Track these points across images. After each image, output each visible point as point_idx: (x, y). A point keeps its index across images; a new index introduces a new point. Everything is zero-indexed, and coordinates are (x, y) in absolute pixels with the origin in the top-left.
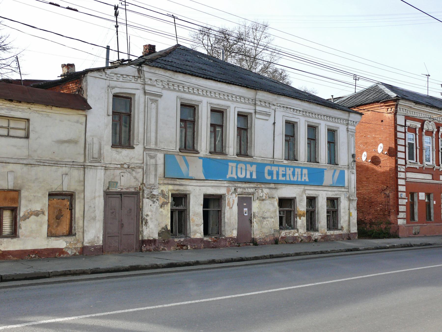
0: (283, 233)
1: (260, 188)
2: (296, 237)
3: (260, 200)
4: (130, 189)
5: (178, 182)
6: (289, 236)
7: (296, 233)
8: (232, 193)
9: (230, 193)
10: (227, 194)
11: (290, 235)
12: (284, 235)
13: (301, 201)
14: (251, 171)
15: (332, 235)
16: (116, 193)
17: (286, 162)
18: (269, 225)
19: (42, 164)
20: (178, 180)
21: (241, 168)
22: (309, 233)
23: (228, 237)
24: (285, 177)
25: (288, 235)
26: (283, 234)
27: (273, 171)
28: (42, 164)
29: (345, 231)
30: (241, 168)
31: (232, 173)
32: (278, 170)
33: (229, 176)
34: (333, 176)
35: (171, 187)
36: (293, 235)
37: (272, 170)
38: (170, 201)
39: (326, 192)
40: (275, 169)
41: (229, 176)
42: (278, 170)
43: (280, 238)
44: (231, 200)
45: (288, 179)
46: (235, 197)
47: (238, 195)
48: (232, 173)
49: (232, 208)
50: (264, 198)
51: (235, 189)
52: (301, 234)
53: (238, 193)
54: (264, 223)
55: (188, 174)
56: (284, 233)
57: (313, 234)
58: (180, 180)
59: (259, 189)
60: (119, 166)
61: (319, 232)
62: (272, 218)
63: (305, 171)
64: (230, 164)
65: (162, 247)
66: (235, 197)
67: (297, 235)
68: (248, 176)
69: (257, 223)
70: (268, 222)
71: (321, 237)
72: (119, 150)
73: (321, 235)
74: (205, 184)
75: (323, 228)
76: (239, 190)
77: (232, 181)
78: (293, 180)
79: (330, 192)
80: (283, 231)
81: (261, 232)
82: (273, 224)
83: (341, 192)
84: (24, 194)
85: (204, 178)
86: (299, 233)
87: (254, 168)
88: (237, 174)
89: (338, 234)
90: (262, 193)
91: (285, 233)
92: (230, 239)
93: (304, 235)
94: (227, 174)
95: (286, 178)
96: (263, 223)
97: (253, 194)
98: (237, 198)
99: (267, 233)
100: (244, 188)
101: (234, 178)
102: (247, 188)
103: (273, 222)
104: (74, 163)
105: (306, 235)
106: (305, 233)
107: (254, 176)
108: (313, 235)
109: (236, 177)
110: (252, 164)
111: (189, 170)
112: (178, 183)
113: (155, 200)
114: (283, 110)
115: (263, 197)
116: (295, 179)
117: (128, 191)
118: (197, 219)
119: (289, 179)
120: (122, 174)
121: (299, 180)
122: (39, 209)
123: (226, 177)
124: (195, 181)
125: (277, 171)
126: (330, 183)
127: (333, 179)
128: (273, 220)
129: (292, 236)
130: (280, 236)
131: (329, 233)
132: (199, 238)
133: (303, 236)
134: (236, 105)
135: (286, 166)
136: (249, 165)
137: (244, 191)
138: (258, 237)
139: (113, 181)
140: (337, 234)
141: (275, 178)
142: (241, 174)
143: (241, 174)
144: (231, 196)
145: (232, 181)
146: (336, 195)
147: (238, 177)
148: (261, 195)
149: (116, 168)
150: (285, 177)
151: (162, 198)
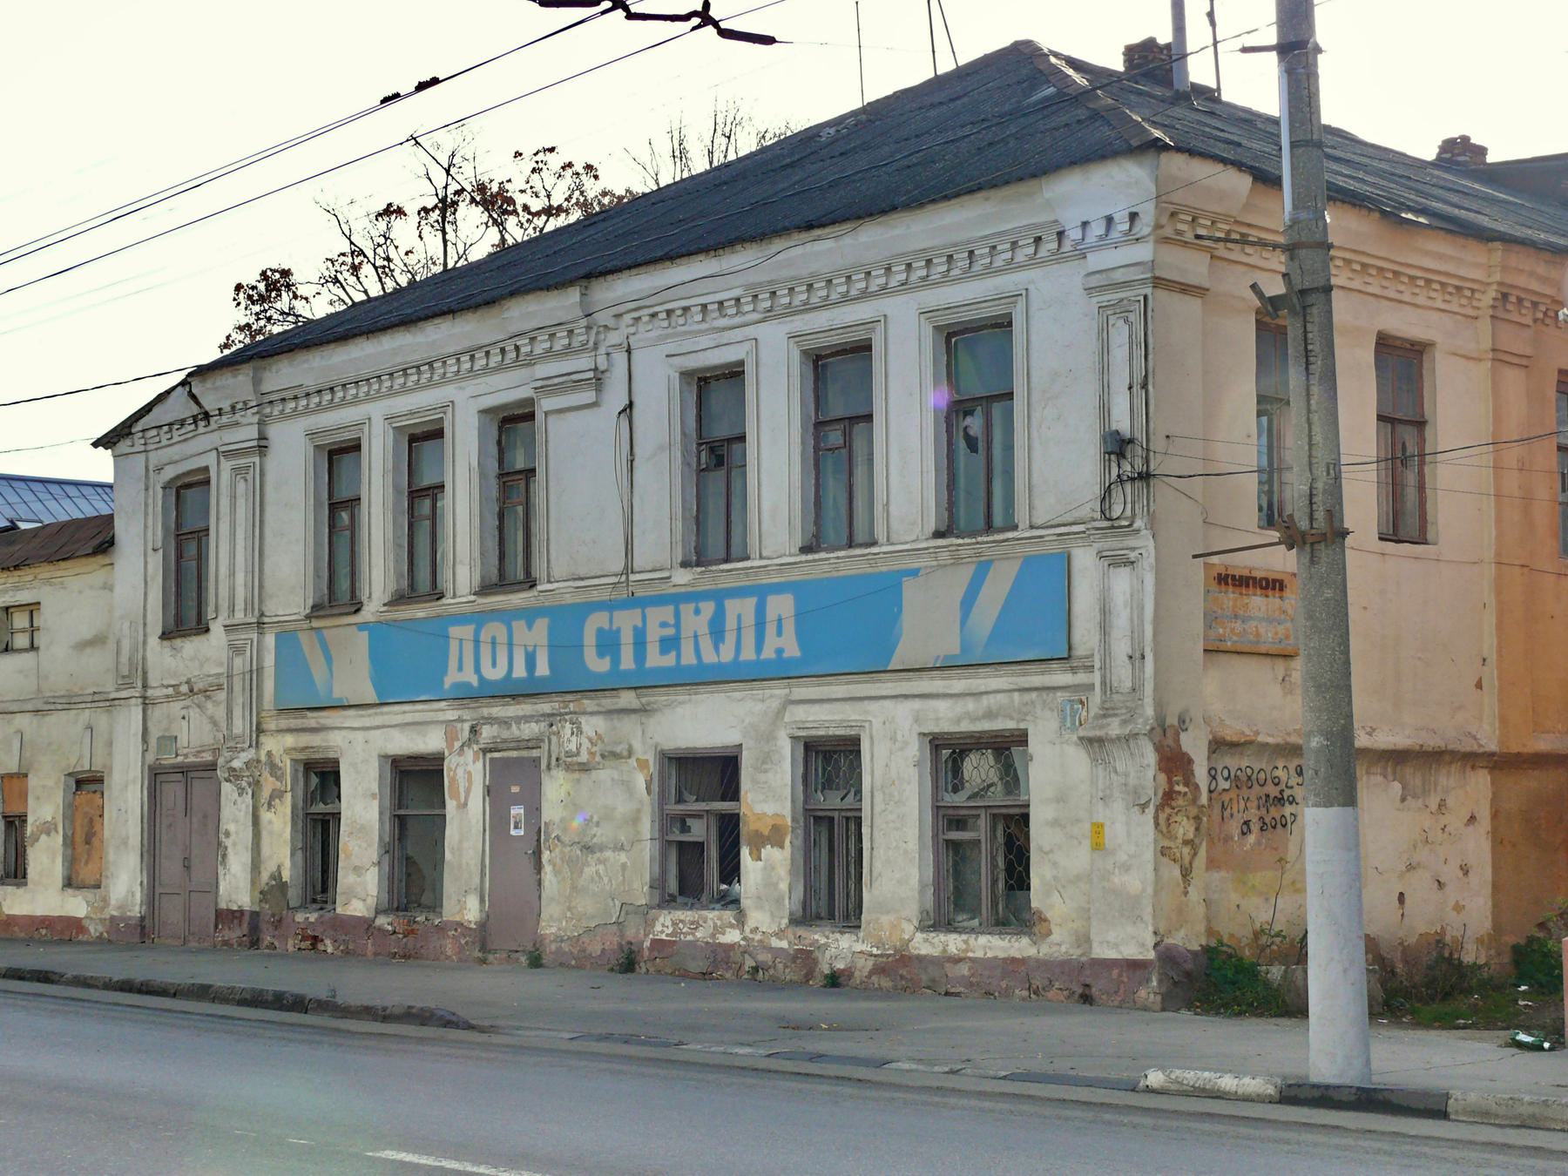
0: (665, 924)
1: (567, 717)
2: (731, 947)
3: (569, 768)
4: (203, 755)
5: (312, 719)
6: (690, 938)
7: (732, 926)
8: (463, 746)
9: (457, 745)
10: (446, 754)
11: (698, 935)
12: (670, 931)
13: (764, 762)
14: (530, 649)
15: (957, 960)
16: (174, 768)
17: (682, 577)
18: (606, 880)
19: (52, 707)
20: (309, 714)
21: (494, 643)
22: (801, 931)
23: (452, 922)
24: (674, 654)
25: (686, 934)
26: (663, 925)
27: (619, 630)
28: (52, 707)
29: (1058, 944)
30: (494, 643)
31: (460, 669)
32: (640, 625)
33: (452, 678)
34: (968, 602)
35: (290, 740)
36: (713, 936)
37: (614, 628)
38: (289, 788)
39: (917, 704)
40: (626, 622)
41: (452, 678)
42: (640, 625)
43: (647, 944)
44: (460, 772)
45: (688, 658)
46: (474, 762)
47: (485, 751)
48: (460, 669)
49: (465, 804)
50: (584, 757)
51: (474, 730)
52: (758, 937)
53: (482, 746)
54: (586, 870)
55: (331, 692)
56: (668, 923)
57: (823, 941)
58: (315, 714)
59: (566, 721)
60: (170, 691)
61: (861, 935)
62: (622, 848)
63: (781, 606)
64: (455, 631)
65: (268, 938)
66: (474, 762)
67: (732, 937)
68: (520, 671)
69: (556, 872)
70: (601, 867)
71: (870, 963)
72: (178, 642)
73: (875, 951)
74: (378, 721)
75: (888, 912)
76: (487, 732)
77: (465, 697)
78: (715, 660)
79: (942, 706)
80: (666, 912)
81: (569, 909)
82: (623, 876)
83: (1034, 695)
84: (32, 781)
85: (371, 697)
86: (747, 929)
87: (537, 635)
88: (477, 670)
89: (1001, 955)
90: (574, 739)
91: (674, 924)
92: (456, 930)
93: (776, 943)
94: (445, 673)
95: (678, 656)
96: (582, 872)
97: (534, 743)
98: (480, 764)
99: (593, 917)
100: (506, 723)
101: (468, 685)
102: (519, 720)
103: (624, 866)
104: (96, 697)
105: (784, 944)
106: (779, 934)
107: (543, 669)
108: (826, 946)
109: (474, 681)
110: (529, 615)
111: (332, 675)
112: (312, 723)
113: (244, 784)
114: (660, 332)
115: (578, 754)
116: (727, 654)
117: (199, 760)
118: (360, 847)
119: (695, 662)
120: (184, 712)
121: (748, 654)
122: (49, 819)
123: (443, 682)
124: (351, 712)
125: (635, 628)
126: (950, 645)
127: (963, 623)
128: (623, 857)
129: (707, 943)
130: (646, 935)
131: (927, 945)
132: (360, 915)
133: (770, 949)
134: (473, 386)
135: (677, 599)
136: (522, 623)
137: (505, 734)
138: (553, 930)
139: (167, 734)
140: (989, 955)
141: (627, 662)
142: (494, 664)
143: (494, 664)
144: (461, 760)
145: (465, 697)
146: (990, 715)
147: (481, 679)
148: (573, 747)
149: (167, 696)
150: (674, 654)
151: (271, 779)
